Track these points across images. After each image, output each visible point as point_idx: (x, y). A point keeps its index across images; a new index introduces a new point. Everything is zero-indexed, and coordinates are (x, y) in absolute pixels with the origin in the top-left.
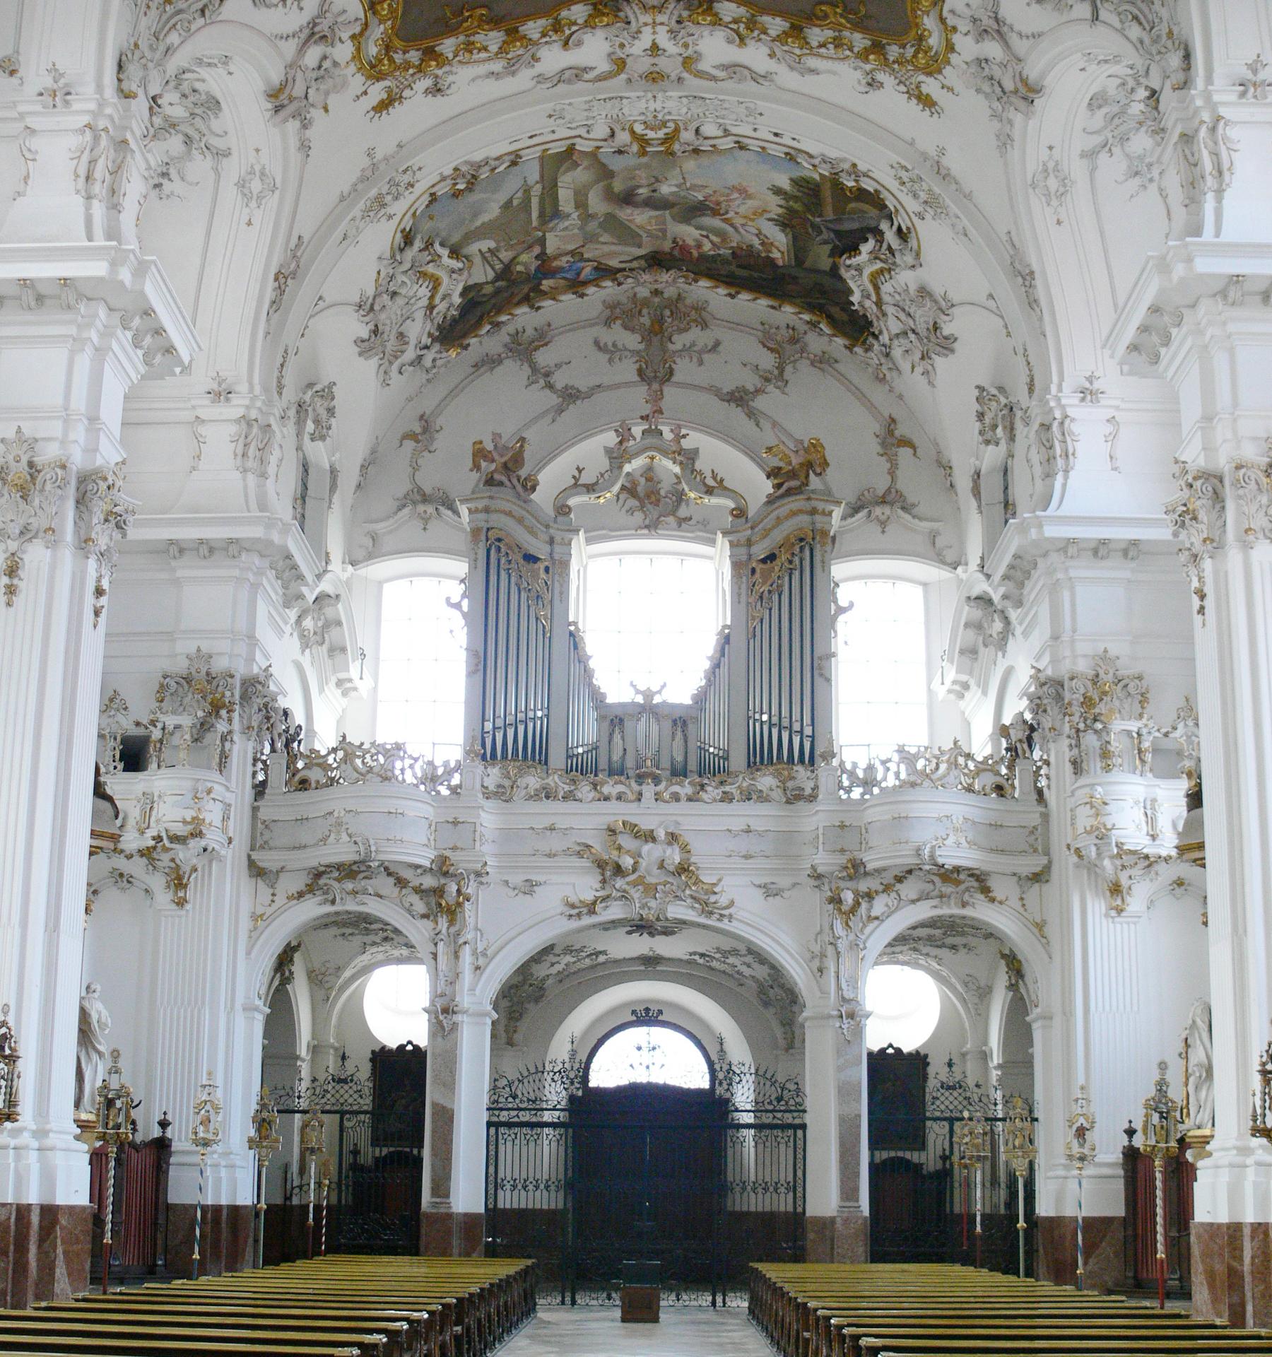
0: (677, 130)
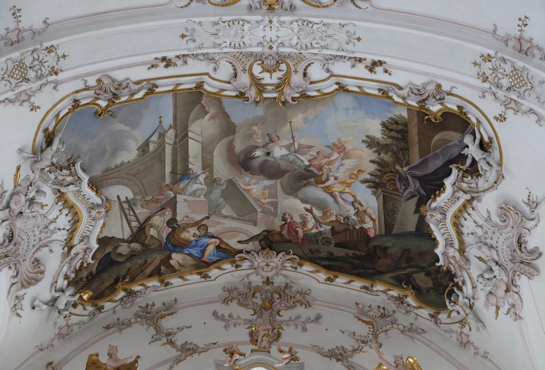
0: (288, 74)
